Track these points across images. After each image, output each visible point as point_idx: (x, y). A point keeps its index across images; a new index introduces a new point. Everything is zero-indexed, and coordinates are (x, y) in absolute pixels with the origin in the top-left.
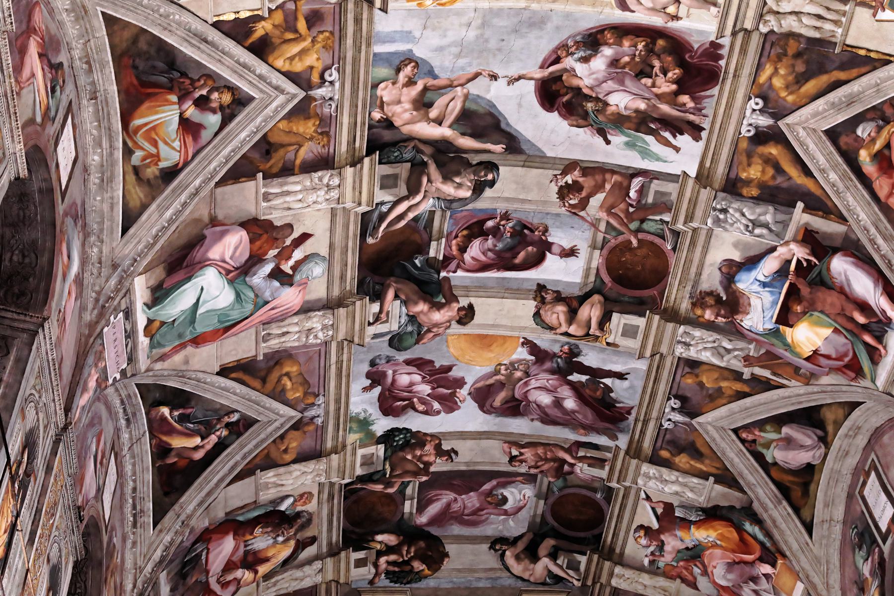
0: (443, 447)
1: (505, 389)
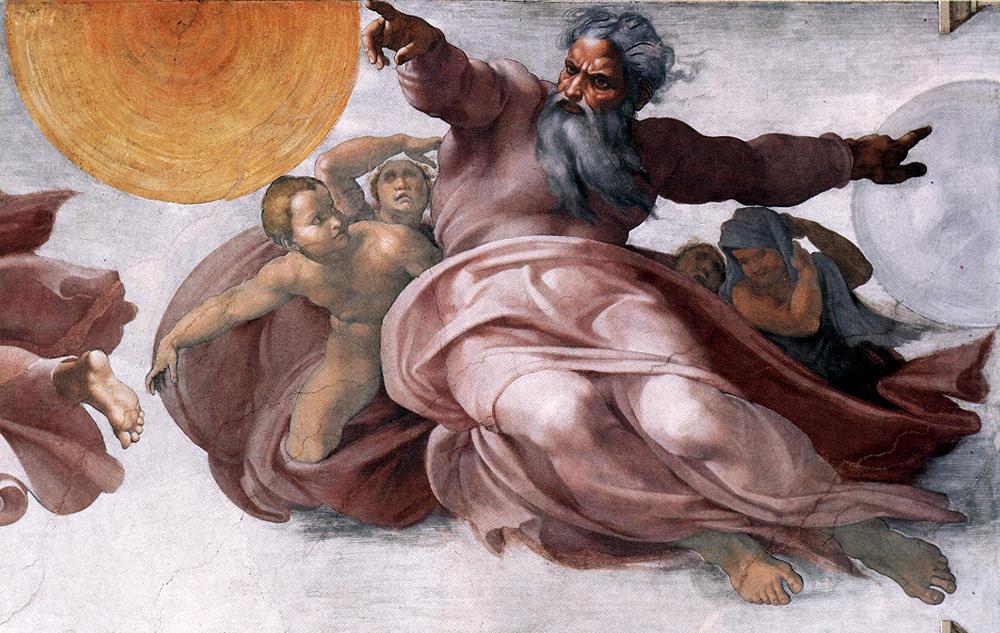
1: (332, 344)
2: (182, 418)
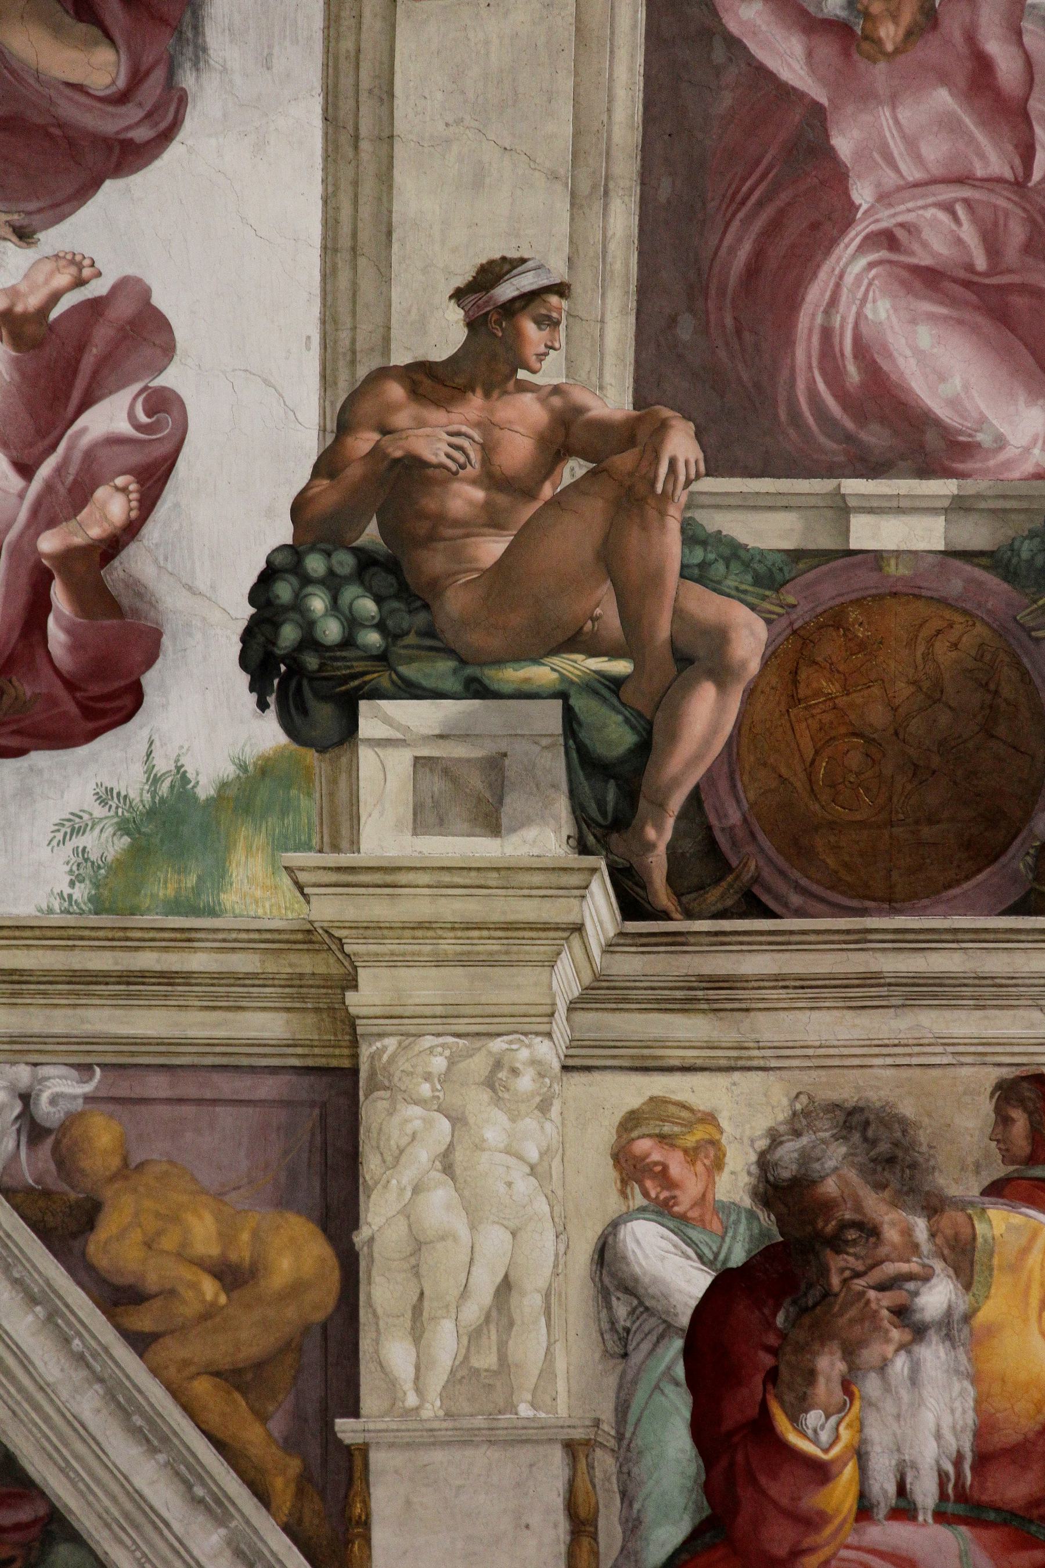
0: (440, 353)
2: (66, 208)
